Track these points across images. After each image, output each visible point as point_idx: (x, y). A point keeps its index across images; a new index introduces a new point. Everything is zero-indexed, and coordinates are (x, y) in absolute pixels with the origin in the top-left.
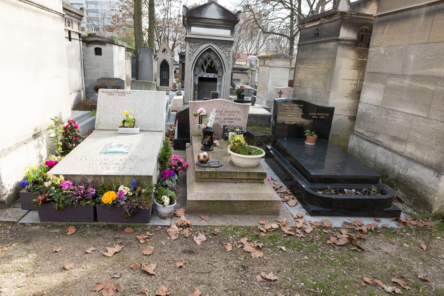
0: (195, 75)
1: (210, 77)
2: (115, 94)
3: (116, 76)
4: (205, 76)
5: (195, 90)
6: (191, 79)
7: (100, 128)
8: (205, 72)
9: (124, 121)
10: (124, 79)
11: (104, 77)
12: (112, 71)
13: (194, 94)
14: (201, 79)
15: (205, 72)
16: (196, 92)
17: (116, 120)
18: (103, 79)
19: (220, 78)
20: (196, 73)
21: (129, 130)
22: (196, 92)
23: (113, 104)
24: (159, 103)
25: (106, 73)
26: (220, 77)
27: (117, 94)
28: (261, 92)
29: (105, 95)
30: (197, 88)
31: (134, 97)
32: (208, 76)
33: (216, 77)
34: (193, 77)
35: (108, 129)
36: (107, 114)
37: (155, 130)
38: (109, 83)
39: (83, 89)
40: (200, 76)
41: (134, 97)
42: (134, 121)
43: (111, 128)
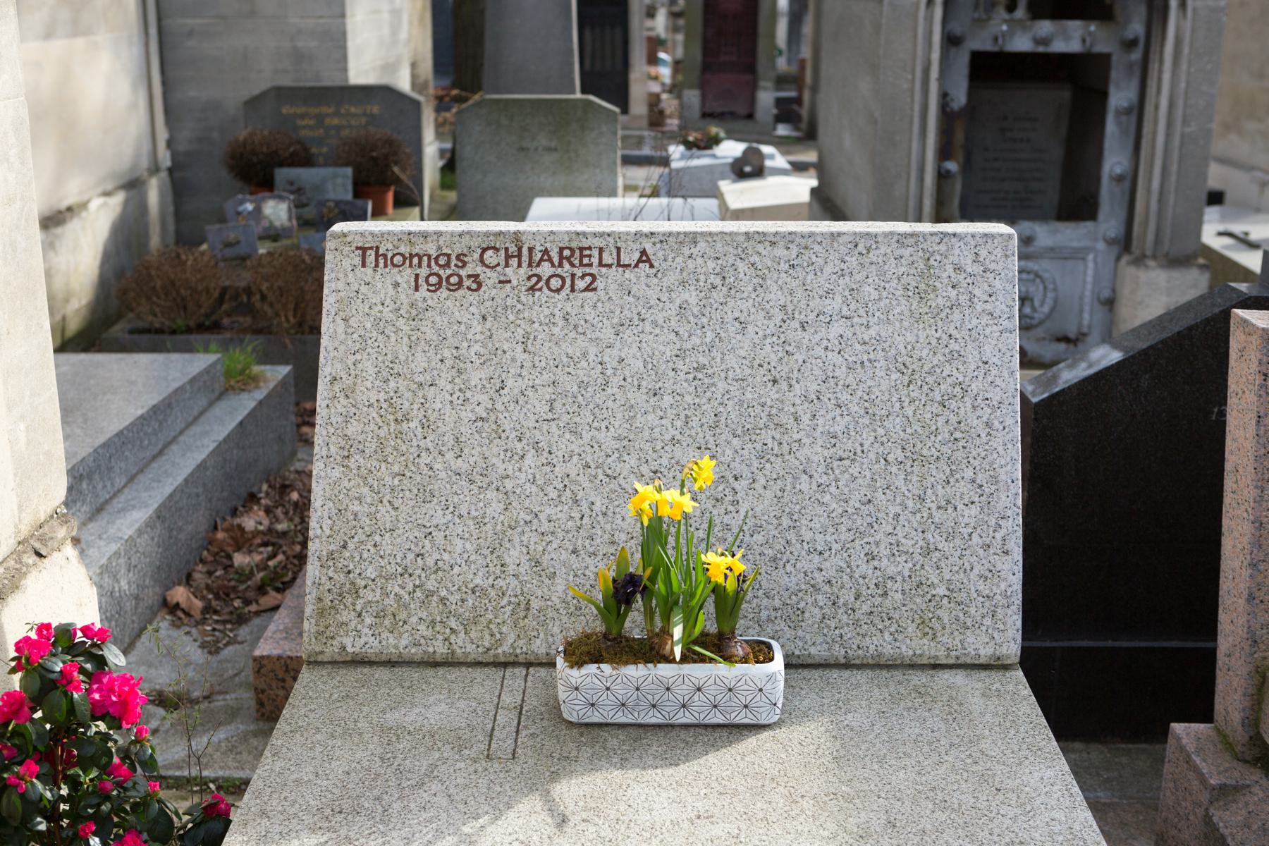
0: (951, 41)
1: (1059, 47)
2: (490, 278)
3: (361, 72)
4: (1022, 43)
5: (944, 152)
6: (926, 71)
7: (353, 646)
8: (1020, 13)
9: (626, 590)
10: (403, 83)
11: (286, 81)
12: (337, 41)
13: (942, 176)
14: (991, 69)
15: (1020, 13)
16: (952, 166)
17: (513, 555)
18: (281, 94)
19: (1136, 55)
20: (957, 28)
21: (682, 692)
22: (952, 166)
23: (476, 376)
24: (953, 357)
25: (299, 57)
26: (1131, 44)
27: (518, 274)
28: (1251, 126)
29: (389, 288)
30: (959, 136)
31: (691, 296)
32: (1045, 41)
33: (1100, 48)
34: (936, 56)
35: (440, 649)
36: (425, 495)
37: (914, 645)
38: (320, 119)
39: (155, 169)
40: (981, 42)
41: (691, 296)
42: (731, 585)
43: (464, 645)
